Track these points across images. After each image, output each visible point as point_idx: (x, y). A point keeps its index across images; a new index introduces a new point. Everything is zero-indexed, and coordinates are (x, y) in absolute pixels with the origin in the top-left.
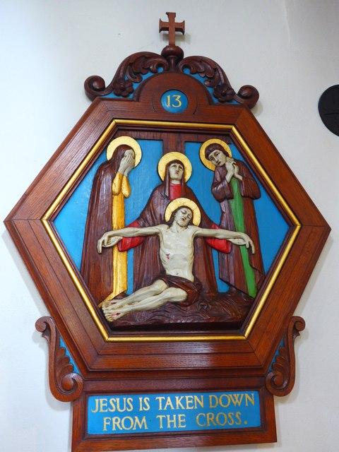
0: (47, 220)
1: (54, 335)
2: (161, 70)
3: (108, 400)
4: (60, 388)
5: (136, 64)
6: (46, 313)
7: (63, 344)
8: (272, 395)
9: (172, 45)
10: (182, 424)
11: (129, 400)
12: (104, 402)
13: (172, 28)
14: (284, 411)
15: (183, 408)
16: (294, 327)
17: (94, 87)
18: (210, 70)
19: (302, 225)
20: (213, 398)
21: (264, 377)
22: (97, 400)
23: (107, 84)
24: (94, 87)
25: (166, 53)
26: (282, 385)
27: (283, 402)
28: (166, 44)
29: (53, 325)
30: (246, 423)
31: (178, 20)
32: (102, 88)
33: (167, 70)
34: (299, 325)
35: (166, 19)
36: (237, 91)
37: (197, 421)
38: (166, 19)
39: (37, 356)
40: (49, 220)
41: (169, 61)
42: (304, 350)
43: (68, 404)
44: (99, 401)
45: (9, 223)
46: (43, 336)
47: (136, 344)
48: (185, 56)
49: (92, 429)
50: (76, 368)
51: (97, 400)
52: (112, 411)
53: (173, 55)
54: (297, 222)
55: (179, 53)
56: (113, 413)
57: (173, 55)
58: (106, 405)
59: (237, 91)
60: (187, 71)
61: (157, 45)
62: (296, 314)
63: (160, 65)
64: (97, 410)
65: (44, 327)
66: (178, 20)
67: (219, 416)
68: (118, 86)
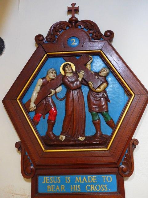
0: (19, 100)
1: (23, 148)
2: (68, 28)
3: (50, 178)
4: (26, 172)
5: (58, 28)
6: (18, 140)
7: (27, 154)
8: (123, 177)
9: (73, 17)
10: (53, 189)
11: (59, 178)
12: (48, 178)
13: (73, 10)
14: (128, 184)
15: (86, 182)
16: (133, 144)
17: (39, 39)
18: (90, 26)
19: (135, 95)
20: (90, 178)
21: (118, 167)
22: (45, 178)
23: (45, 37)
24: (39, 39)
25: (71, 20)
26: (126, 172)
27: (126, 180)
28: (70, 16)
29: (22, 146)
30: (110, 190)
31: (76, 6)
32: (44, 39)
33: (70, 28)
34: (136, 142)
35: (71, 6)
36: (103, 34)
37: (86, 187)
38: (71, 6)
39: (16, 157)
40: (19, 100)
41: (72, 25)
42: (138, 155)
43: (30, 179)
44: (46, 178)
45: (4, 101)
46: (18, 150)
47: (75, 152)
48: (79, 21)
49: (41, 190)
50: (32, 165)
51: (45, 178)
52: (51, 182)
53: (73, 22)
54: (133, 94)
55: (77, 20)
56: (50, 183)
57: (73, 22)
58: (49, 180)
59: (103, 34)
60: (79, 27)
61: (66, 18)
62: (133, 138)
63: (68, 26)
64: (44, 182)
65: (18, 146)
66: (76, 6)
67: (88, 186)
68: (48, 38)
